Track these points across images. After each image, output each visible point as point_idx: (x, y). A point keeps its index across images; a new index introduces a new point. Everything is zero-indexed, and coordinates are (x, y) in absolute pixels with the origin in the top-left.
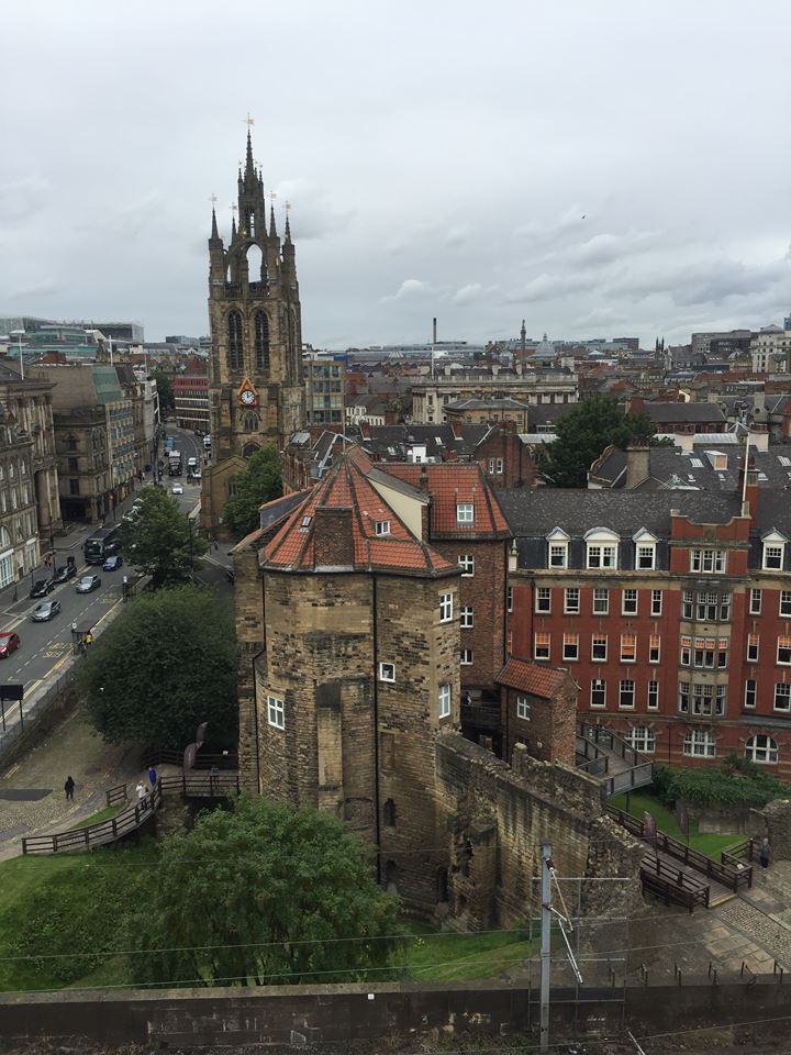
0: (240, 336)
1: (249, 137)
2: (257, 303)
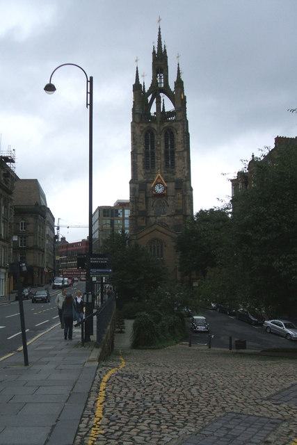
0: (153, 147)
1: (160, 29)
2: (166, 124)
